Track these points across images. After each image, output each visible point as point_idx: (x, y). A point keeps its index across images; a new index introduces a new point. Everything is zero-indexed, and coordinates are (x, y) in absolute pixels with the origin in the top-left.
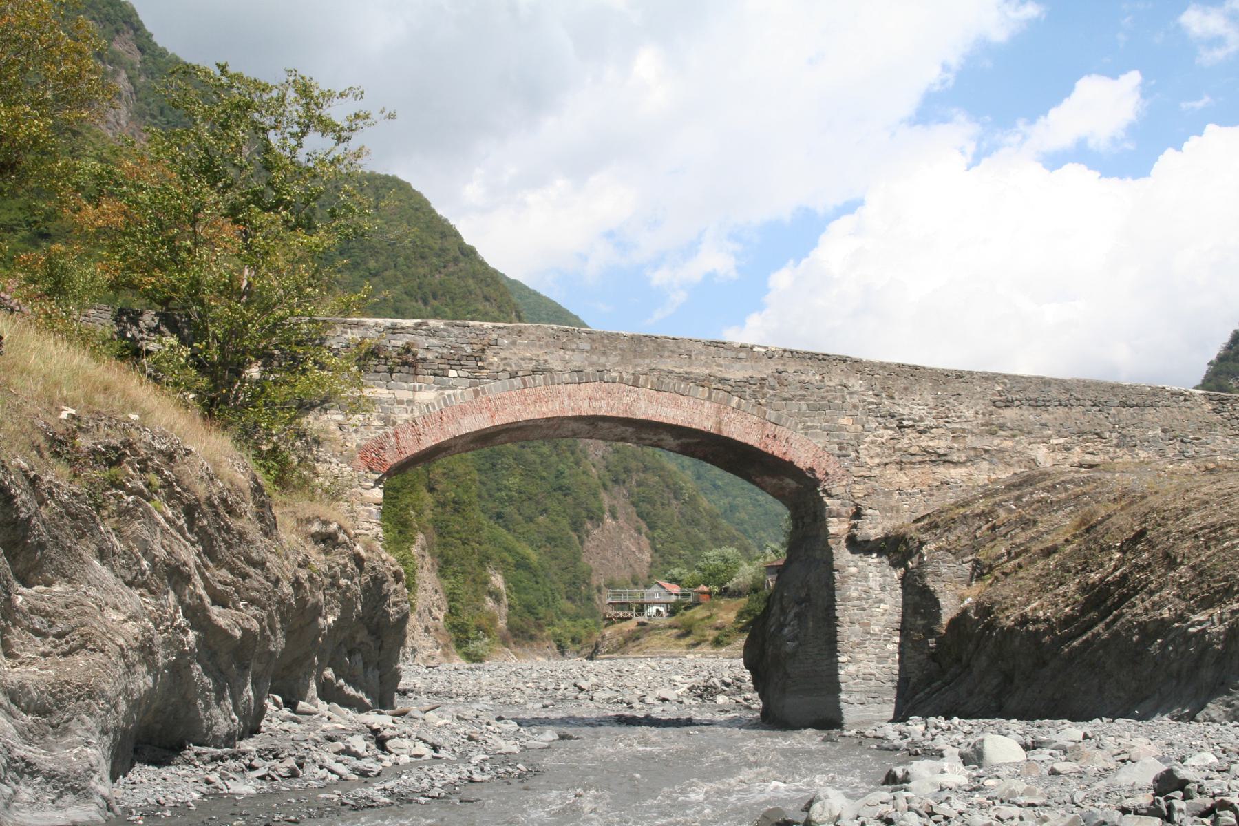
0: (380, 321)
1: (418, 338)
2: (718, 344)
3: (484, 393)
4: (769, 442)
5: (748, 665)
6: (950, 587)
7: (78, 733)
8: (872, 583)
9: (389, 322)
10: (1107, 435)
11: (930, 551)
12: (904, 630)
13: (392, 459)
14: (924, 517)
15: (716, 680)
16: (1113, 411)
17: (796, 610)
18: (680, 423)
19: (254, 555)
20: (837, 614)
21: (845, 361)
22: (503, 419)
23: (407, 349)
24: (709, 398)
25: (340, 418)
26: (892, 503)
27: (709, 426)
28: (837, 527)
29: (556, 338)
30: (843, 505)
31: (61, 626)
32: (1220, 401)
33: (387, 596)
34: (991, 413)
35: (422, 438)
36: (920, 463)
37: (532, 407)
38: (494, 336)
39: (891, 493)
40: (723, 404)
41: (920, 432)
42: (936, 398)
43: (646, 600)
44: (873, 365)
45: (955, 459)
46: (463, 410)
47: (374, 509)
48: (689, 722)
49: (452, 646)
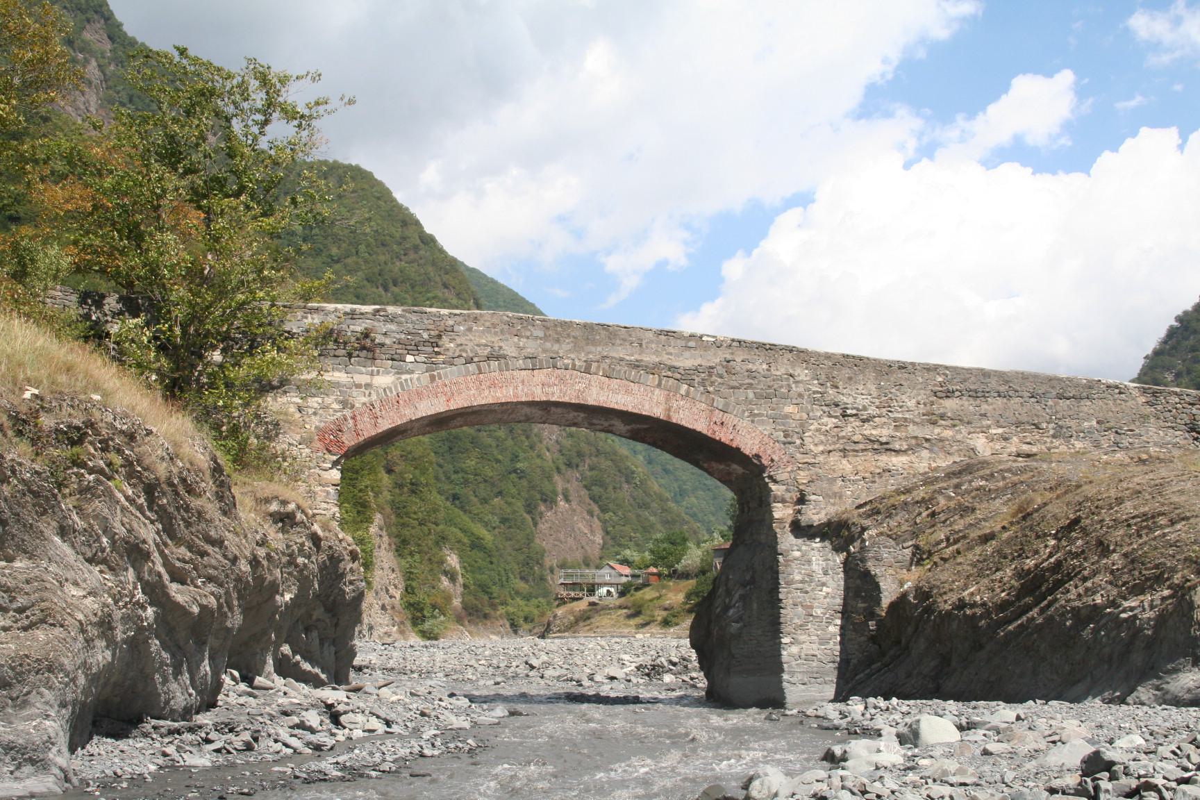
0: (339, 306)
1: (376, 324)
2: (667, 333)
3: (440, 378)
4: (716, 428)
5: (693, 646)
6: (891, 571)
7: (38, 705)
8: (814, 567)
9: (348, 307)
10: (1044, 425)
11: (871, 537)
12: (845, 613)
13: (349, 440)
14: (865, 504)
15: (663, 659)
16: (1050, 403)
17: (741, 592)
18: (630, 409)
19: (212, 533)
20: (781, 596)
21: (791, 351)
22: (458, 403)
23: (366, 335)
24: (659, 385)
26: (836, 489)
27: (658, 412)
28: (782, 512)
29: (510, 324)
30: (788, 490)
31: (21, 601)
32: (1154, 394)
33: (343, 575)
34: (932, 403)
35: (380, 420)
36: (863, 450)
37: (487, 392)
38: (451, 322)
39: (834, 479)
40: (671, 392)
41: (864, 421)
42: (879, 388)
43: (597, 581)
44: (818, 355)
45: (897, 447)
46: (419, 395)
47: (331, 490)
48: (636, 700)
49: (408, 624)
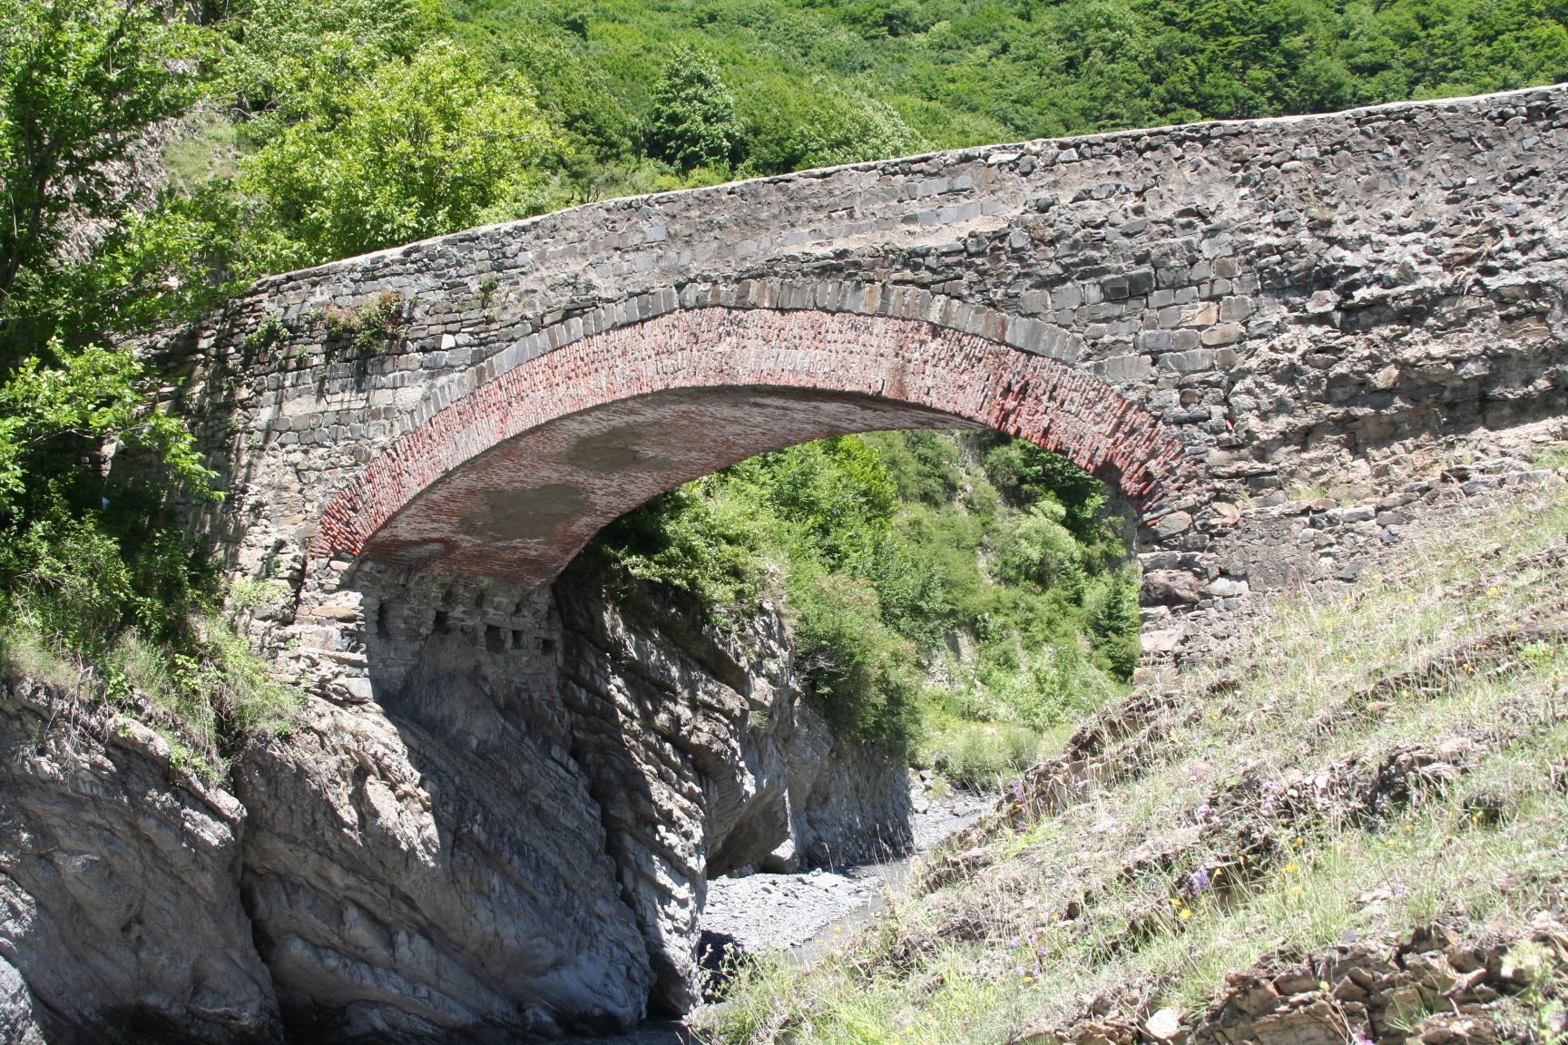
1: (404, 280)
9: (363, 260)
13: (363, 525)
18: (820, 385)
25: (298, 457)
26: (1286, 551)
27: (875, 379)
42: (1457, 196)
47: (334, 629)
